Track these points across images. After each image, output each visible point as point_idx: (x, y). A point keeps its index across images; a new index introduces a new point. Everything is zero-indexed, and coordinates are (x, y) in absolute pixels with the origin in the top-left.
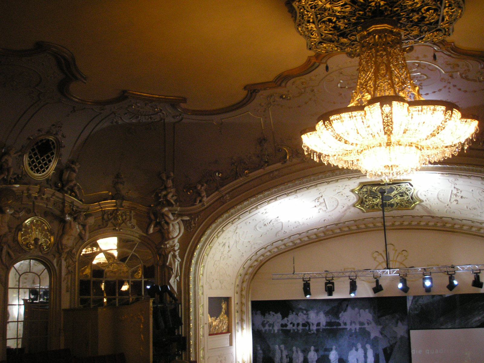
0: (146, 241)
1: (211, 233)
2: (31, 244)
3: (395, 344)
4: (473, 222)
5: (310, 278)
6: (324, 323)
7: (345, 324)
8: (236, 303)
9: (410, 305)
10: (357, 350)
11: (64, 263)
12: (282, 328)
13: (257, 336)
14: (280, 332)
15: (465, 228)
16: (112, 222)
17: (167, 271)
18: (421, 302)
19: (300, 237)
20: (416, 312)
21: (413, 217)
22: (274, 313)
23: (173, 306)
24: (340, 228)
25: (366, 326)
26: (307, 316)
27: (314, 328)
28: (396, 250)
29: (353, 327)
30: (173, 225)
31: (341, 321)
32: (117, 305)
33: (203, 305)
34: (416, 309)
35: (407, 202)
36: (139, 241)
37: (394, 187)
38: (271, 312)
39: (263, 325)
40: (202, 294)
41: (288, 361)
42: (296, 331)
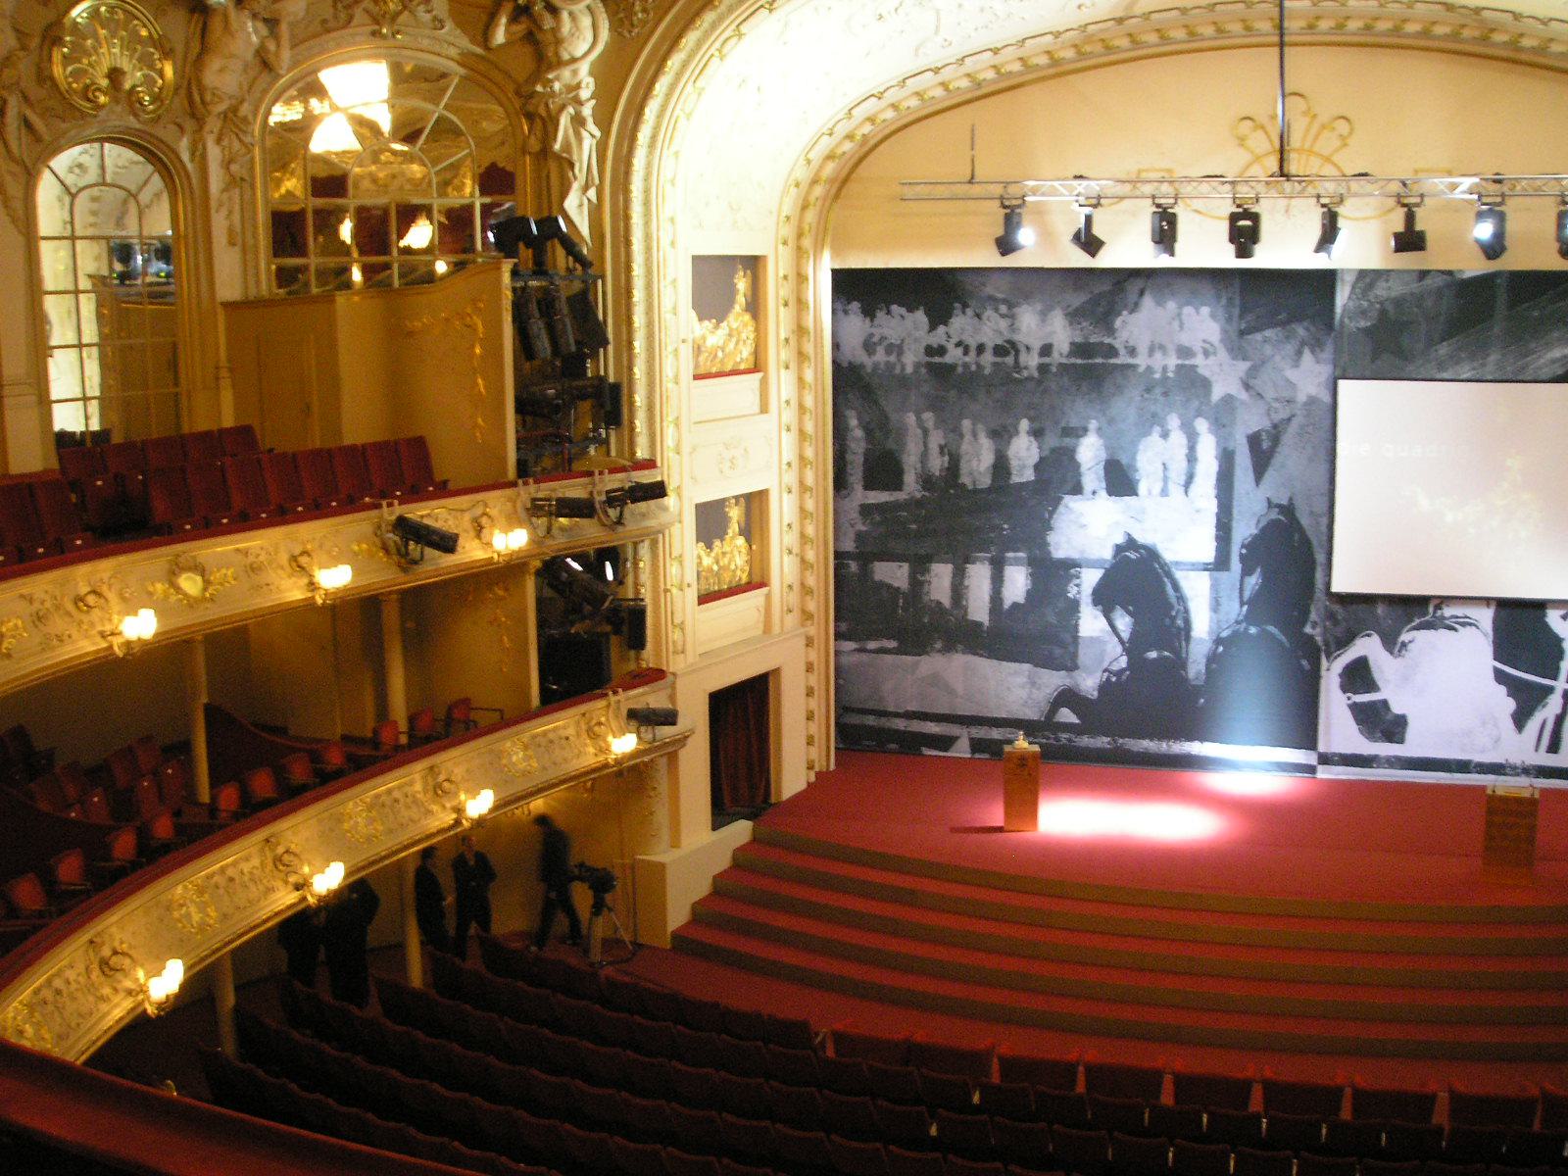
0: (482, 71)
1: (699, 44)
2: (99, 90)
6: (1065, 348)
8: (781, 274)
10: (1165, 435)
11: (214, 153)
13: (848, 381)
14: (923, 371)
16: (367, 11)
17: (555, 168)
18: (1381, 290)
19: (997, 60)
20: (1363, 324)
22: (903, 311)
23: (577, 286)
24: (1130, 35)
27: (1032, 361)
29: (1158, 361)
30: (571, 14)
31: (1118, 344)
32: (396, 283)
33: (675, 280)
34: (1363, 313)
36: (462, 71)
38: (894, 308)
39: (869, 346)
40: (673, 244)
41: (946, 465)
42: (973, 368)
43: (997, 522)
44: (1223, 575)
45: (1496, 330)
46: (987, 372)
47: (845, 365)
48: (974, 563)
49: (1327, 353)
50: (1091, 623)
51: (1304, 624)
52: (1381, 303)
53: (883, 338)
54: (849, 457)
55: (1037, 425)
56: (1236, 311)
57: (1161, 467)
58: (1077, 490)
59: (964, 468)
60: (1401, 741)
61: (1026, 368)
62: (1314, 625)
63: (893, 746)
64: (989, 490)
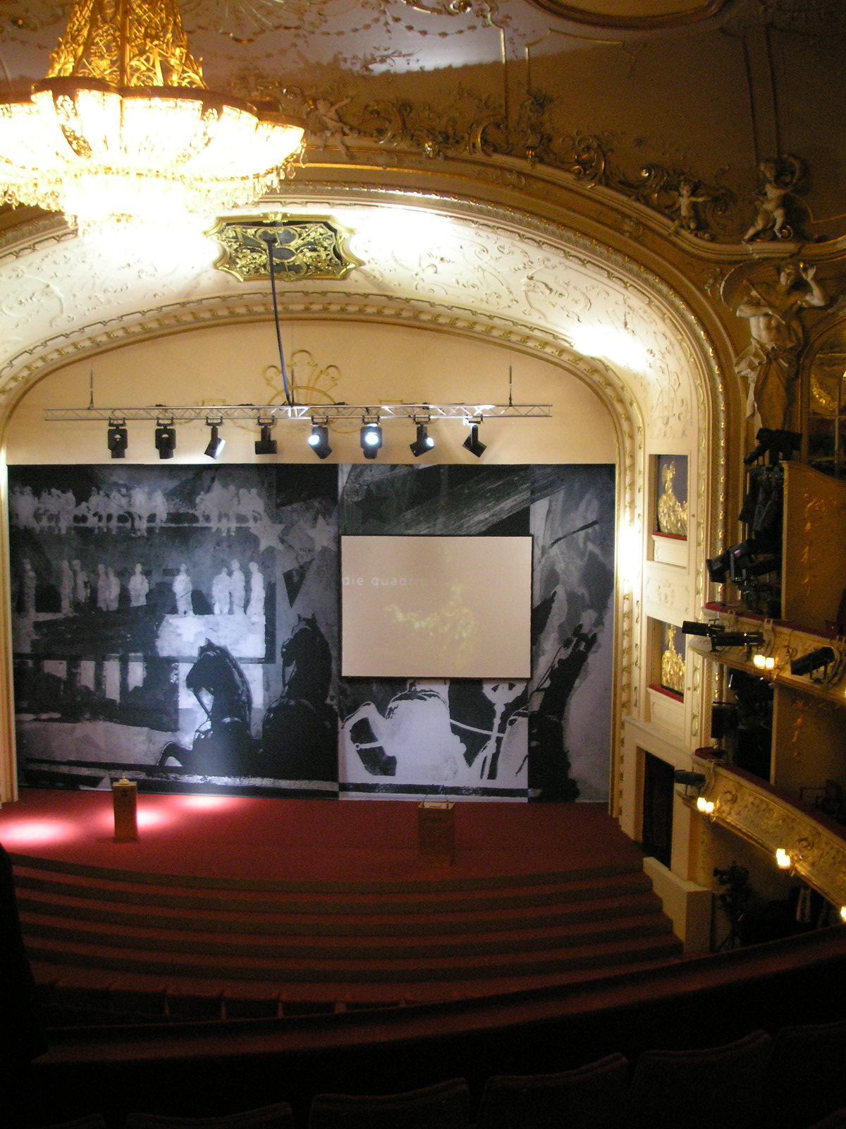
3: (310, 562)
4: (474, 313)
5: (124, 419)
6: (165, 516)
7: (207, 519)
9: (345, 481)
10: (230, 574)
12: (76, 525)
14: (73, 532)
15: (460, 324)
18: (367, 477)
19: (107, 329)
20: (356, 499)
21: (348, 295)
22: (59, 492)
25: (251, 524)
26: (127, 499)
27: (143, 525)
28: (316, 365)
29: (224, 525)
31: (198, 513)
34: (357, 492)
35: (328, 262)
37: (292, 231)
38: (53, 490)
39: (37, 516)
42: (105, 530)
43: (122, 632)
44: (271, 667)
45: (442, 502)
46: (114, 533)
47: (22, 528)
48: (108, 660)
49: (333, 520)
50: (186, 700)
51: (325, 699)
52: (368, 486)
53: (46, 511)
54: (26, 590)
55: (147, 568)
56: (274, 491)
57: (228, 595)
58: (174, 610)
59: (101, 596)
60: (393, 774)
61: (139, 530)
62: (332, 700)
63: (60, 785)
64: (118, 611)
